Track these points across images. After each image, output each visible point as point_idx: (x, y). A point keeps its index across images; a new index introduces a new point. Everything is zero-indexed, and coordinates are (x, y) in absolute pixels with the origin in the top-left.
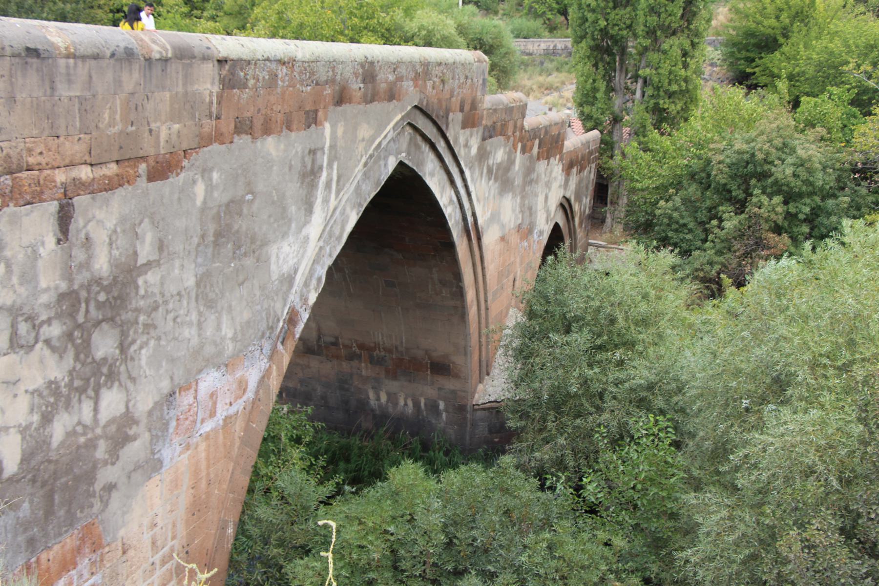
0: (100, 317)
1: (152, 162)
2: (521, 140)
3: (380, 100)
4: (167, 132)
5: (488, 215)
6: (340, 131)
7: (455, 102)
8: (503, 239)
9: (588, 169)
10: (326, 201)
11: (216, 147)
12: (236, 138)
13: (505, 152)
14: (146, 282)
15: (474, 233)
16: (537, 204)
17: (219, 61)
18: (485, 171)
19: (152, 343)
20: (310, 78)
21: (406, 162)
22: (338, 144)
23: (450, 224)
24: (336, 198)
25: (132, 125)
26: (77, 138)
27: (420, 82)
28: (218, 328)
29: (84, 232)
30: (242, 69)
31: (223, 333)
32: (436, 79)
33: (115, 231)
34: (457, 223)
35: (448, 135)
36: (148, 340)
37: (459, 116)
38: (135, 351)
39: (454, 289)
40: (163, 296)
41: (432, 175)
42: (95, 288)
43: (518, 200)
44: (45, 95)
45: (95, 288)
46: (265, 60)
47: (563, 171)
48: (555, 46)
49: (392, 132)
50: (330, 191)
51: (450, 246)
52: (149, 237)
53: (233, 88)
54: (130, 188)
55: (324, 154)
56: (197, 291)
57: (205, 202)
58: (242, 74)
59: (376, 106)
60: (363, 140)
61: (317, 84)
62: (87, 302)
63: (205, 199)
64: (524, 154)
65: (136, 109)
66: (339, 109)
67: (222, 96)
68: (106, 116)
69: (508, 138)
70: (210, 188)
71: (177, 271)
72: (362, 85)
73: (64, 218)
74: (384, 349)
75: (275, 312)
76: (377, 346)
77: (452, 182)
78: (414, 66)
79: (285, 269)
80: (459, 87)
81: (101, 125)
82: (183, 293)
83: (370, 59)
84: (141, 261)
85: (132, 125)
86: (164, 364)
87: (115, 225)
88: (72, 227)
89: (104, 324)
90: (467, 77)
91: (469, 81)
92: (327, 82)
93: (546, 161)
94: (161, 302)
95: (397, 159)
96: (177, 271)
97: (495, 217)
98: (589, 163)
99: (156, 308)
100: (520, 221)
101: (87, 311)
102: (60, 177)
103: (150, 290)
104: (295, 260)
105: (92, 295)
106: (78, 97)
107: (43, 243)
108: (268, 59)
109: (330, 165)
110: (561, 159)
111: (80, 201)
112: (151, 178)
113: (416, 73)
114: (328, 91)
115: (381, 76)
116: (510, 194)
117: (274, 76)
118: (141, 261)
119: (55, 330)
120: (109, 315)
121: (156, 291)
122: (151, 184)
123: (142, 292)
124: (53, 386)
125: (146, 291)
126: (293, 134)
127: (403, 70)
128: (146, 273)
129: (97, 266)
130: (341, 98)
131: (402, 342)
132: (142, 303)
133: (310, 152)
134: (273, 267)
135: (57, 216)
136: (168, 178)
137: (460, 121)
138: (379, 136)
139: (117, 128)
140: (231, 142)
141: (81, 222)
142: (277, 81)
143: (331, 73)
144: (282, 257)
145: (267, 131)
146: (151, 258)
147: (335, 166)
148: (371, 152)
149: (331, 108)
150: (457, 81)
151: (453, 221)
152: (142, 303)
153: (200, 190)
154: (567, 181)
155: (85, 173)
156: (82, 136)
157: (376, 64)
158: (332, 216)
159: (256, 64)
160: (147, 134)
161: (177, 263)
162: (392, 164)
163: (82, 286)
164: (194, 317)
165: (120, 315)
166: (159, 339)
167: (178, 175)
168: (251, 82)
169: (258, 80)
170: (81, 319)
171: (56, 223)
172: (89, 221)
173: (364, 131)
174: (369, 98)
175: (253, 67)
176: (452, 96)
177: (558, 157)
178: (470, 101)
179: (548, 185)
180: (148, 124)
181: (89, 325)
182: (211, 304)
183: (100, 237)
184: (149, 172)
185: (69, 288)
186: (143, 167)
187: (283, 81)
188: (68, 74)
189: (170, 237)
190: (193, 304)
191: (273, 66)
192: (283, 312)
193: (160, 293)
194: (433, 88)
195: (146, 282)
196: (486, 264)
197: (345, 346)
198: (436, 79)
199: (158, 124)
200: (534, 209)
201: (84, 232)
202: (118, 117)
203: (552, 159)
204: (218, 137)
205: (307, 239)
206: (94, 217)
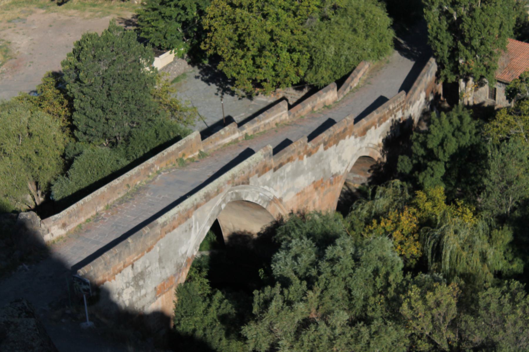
11: (161, 240)
18: (278, 179)
79: (183, 252)
100: (314, 179)
102: (132, 261)
109: (195, 223)
111: (135, 263)
112: (147, 252)
117: (174, 218)
119: (132, 283)
124: (133, 292)
127: (222, 184)
130: (196, 207)
145: (174, 228)
147: (197, 223)
151: (262, 202)
155: (136, 258)
164: (159, 272)
182: (164, 268)
186: (146, 252)
204: (162, 237)
205: (190, 243)
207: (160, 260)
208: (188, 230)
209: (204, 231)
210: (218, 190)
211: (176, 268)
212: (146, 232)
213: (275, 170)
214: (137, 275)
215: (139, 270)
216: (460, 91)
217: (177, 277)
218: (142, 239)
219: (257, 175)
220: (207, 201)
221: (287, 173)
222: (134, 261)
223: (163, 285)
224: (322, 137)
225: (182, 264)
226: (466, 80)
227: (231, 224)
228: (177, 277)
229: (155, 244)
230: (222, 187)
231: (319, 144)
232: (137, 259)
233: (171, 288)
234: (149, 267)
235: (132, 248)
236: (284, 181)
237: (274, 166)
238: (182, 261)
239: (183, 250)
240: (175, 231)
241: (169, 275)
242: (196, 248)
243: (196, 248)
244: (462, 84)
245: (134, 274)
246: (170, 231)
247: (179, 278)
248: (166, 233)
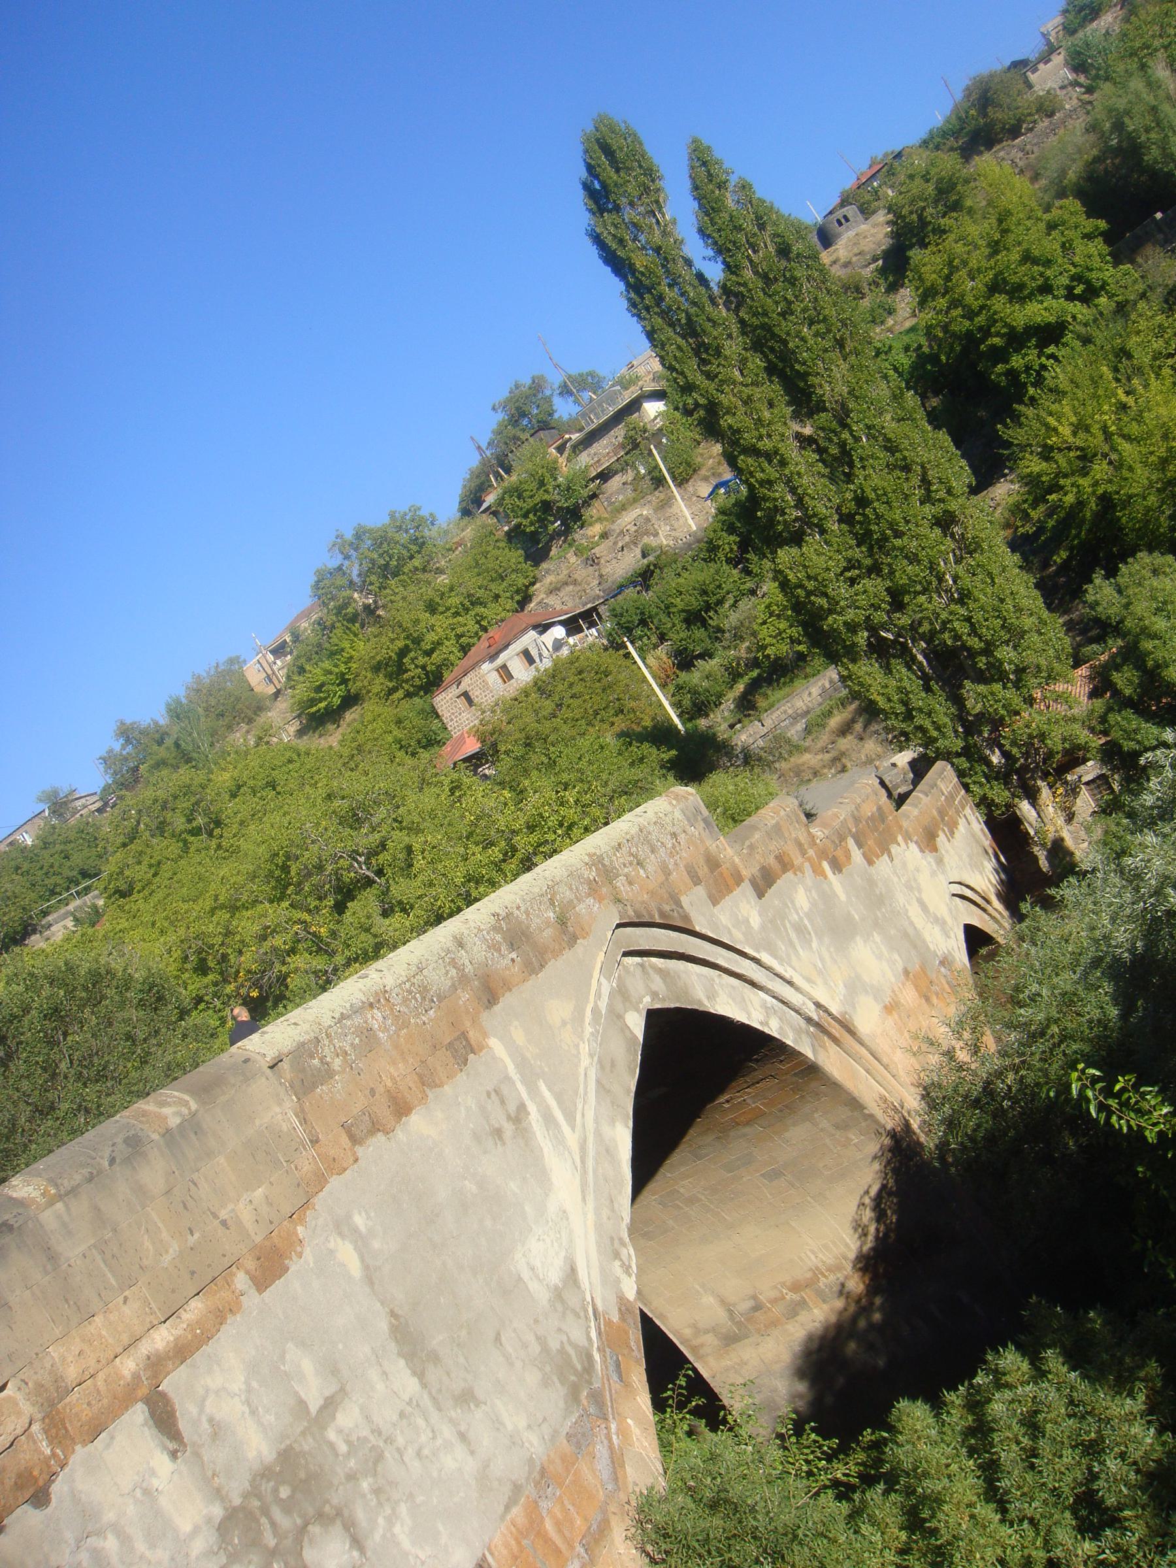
0: (299, 1521)
1: (251, 1264)
2: (823, 854)
3: (557, 954)
4: (249, 1207)
5: (841, 989)
6: (519, 1036)
7: (679, 876)
8: (889, 1009)
9: (962, 821)
10: (559, 1141)
11: (335, 1182)
12: (360, 1150)
13: (808, 890)
14: (340, 1431)
15: (833, 1027)
16: (912, 923)
17: (271, 1067)
18: (793, 936)
19: (403, 1509)
20: (424, 998)
21: (658, 1006)
22: (528, 1055)
23: (789, 1042)
24: (573, 1129)
25: (192, 1233)
26: (121, 1299)
27: (604, 890)
28: (497, 1423)
29: (204, 1419)
30: (312, 1057)
31: (510, 1427)
32: (626, 870)
33: (249, 1390)
34: (798, 1031)
35: (698, 929)
36: (393, 1509)
37: (700, 891)
38: (384, 1536)
39: (863, 1124)
40: (380, 1434)
41: (712, 996)
42: (267, 1487)
43: (877, 938)
44: (46, 1273)
45: (267, 1487)
46: (340, 1021)
47: (922, 851)
48: (831, 681)
49: (603, 980)
50: (557, 1125)
51: (811, 1070)
52: (307, 1366)
53: (314, 1086)
54: (238, 1317)
55: (514, 1083)
56: (430, 1393)
57: (366, 1267)
58: (316, 1062)
59: (555, 967)
60: (564, 1023)
61: (441, 998)
62: (265, 1511)
63: (362, 1260)
64: (840, 871)
65: (185, 1207)
66: (497, 1008)
67: (303, 1111)
68: (147, 1244)
69: (801, 869)
70: (360, 1241)
71: (380, 1386)
72: (514, 955)
73: (164, 1419)
74: (829, 1270)
75: (575, 1346)
76: (816, 1273)
77: (753, 984)
78: (580, 876)
79: (555, 1276)
80: (671, 855)
81: (145, 1262)
82: (409, 1409)
83: (503, 914)
84: (314, 1406)
85: (192, 1233)
86: (441, 1527)
87: (247, 1383)
88: (182, 1425)
89: (310, 1527)
90: (674, 835)
91: (682, 838)
92: (454, 988)
93: (885, 856)
94: (382, 1444)
95: (637, 1010)
96: (380, 1386)
97: (855, 986)
98: (958, 812)
99: (379, 1457)
100: (900, 966)
101: (273, 1524)
102: (128, 1366)
103: (354, 1438)
104: (563, 1254)
105: (269, 1498)
106: (94, 1246)
107: (153, 1473)
108: (343, 1017)
109: (533, 1090)
110: (908, 838)
112: (262, 1283)
113: (589, 882)
114: (464, 996)
115: (536, 922)
116: (859, 940)
117: (368, 1033)
118: (314, 1406)
120: (311, 1511)
121: (365, 1432)
122: (266, 1294)
123: (343, 1448)
125: (349, 1443)
126: (447, 1088)
128: (334, 1418)
129: (251, 1454)
130: (490, 992)
131: (847, 1245)
132: (352, 1463)
133: (489, 1095)
134: (533, 1286)
135: (151, 1422)
136: (288, 1269)
137: (705, 896)
138: (588, 1002)
139: (171, 1251)
140: (356, 1160)
141: (193, 1410)
142: (375, 1036)
143: (453, 972)
144: (538, 1264)
145: (401, 1109)
146: (327, 1393)
148: (589, 1030)
149: (485, 1016)
150: (662, 851)
151: (791, 1035)
152: (352, 1463)
153: (347, 1255)
154: (940, 861)
155: (161, 1339)
156: (127, 1293)
157: (516, 912)
158: (583, 1162)
159: (328, 1036)
160: (221, 1230)
161: (374, 1374)
162: (637, 1025)
163: (246, 1496)
164: (447, 1432)
165: (328, 1501)
166: (411, 1496)
167: (300, 1255)
168: (337, 1063)
169: (346, 1053)
170: (271, 1542)
171: (155, 1431)
172: (204, 1400)
173: (558, 1010)
174: (536, 964)
175: (327, 1043)
176: (667, 873)
177: (900, 838)
178: (702, 862)
179: (912, 886)
180: (215, 1216)
181: (288, 1542)
182: (467, 1398)
183: (230, 1410)
184: (253, 1278)
185: (226, 1509)
186: (241, 1280)
187: (386, 1030)
188: (64, 1225)
189: (340, 1346)
190: (435, 1416)
191: (358, 1020)
192: (590, 1339)
193: (373, 1431)
194: (630, 883)
195: (340, 1431)
196: (885, 1060)
197: (774, 1301)
198: (626, 870)
199: (230, 1206)
200: (911, 931)
201: (204, 1419)
202: (165, 1235)
203: (894, 849)
204: (336, 1167)
206: (207, 1391)
207: (409, 1341)
208: (508, 1129)
209: (608, 1151)
210: (562, 921)
211: (556, 1395)
212: (172, 1115)
213: (760, 894)
214: (254, 1492)
215: (257, 1446)
216: (1032, 833)
217: (601, 1450)
218: (154, 1173)
219: (700, 891)
220: (534, 966)
221: (807, 915)
222: (157, 1365)
223: (533, 1526)
224: (836, 816)
225: (590, 1357)
226: (1032, 796)
227: (709, 1300)
228: (601, 1450)
229: (296, 1215)
230: (571, 905)
231: (842, 839)
232: (181, 1352)
233: (597, 1537)
234: (330, 1404)
235: (72, 1251)
236: (815, 945)
237: (749, 871)
238: (577, 1335)
239: (539, 1258)
240: (416, 1121)
241: (535, 1445)
242: (617, 1255)
243: (617, 1255)
244: (1025, 808)
245: (218, 1494)
246: (376, 1127)
247: (617, 1461)
248: (355, 1140)
